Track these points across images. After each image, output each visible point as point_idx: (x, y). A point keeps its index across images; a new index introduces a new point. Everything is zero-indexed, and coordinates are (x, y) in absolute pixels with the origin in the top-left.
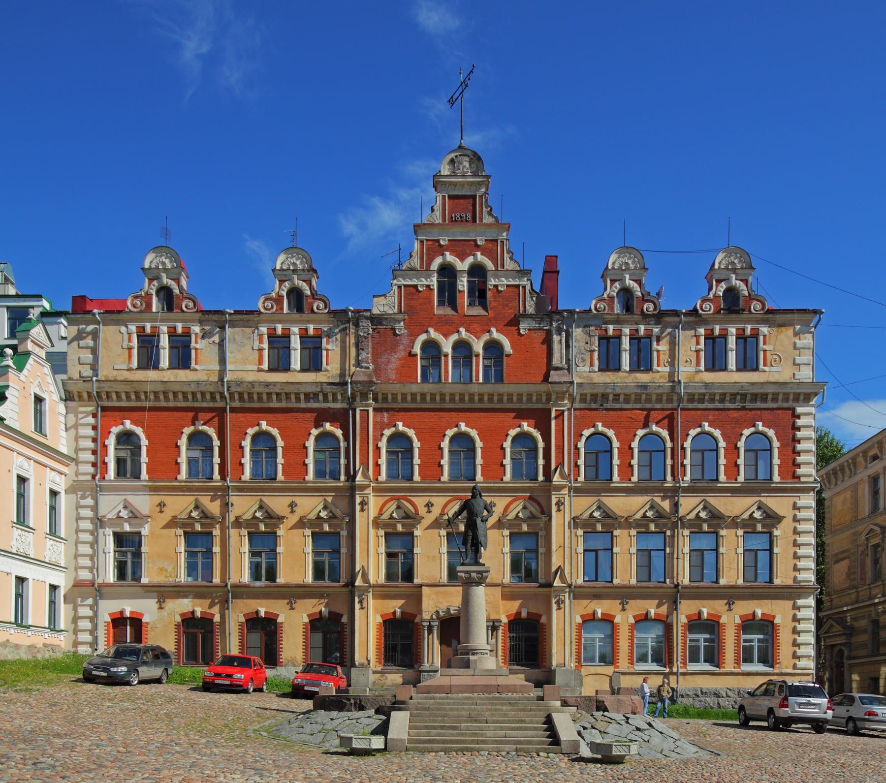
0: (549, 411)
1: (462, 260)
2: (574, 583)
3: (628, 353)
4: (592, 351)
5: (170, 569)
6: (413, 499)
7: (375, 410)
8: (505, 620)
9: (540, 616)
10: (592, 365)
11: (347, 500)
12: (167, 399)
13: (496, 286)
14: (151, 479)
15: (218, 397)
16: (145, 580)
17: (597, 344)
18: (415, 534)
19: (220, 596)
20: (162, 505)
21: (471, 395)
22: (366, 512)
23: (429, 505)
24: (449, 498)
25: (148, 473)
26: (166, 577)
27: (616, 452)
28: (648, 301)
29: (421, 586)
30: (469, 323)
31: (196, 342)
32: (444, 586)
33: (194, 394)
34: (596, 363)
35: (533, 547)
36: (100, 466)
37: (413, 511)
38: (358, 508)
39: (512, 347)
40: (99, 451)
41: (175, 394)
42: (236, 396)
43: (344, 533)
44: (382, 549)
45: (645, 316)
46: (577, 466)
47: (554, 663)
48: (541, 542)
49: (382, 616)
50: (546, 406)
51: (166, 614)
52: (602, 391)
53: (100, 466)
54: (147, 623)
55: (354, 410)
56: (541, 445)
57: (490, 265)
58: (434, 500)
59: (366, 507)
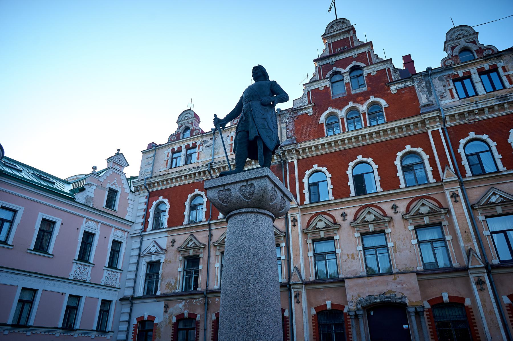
0: (427, 133)
1: (345, 69)
2: (490, 263)
3: (480, 84)
4: (451, 90)
5: (173, 284)
6: (331, 213)
7: (298, 160)
8: (427, 306)
9: (464, 299)
10: (453, 97)
11: (284, 221)
12: (182, 180)
13: (369, 74)
14: (169, 227)
15: (207, 173)
16: (158, 293)
17: (452, 84)
19: (201, 300)
20: (173, 241)
21: (363, 136)
23: (344, 215)
24: (357, 208)
25: (168, 224)
26: (171, 289)
28: (485, 50)
29: (342, 281)
30: (355, 98)
31: (199, 149)
32: (363, 277)
33: (195, 174)
34: (455, 95)
36: (145, 224)
37: (332, 221)
38: (290, 224)
40: (146, 217)
41: (185, 176)
42: (216, 170)
43: (283, 245)
44: (311, 254)
45: (487, 58)
46: (462, 168)
48: (446, 230)
49: (315, 308)
51: (168, 316)
52: (468, 110)
53: (145, 224)
54: (157, 324)
55: (285, 164)
56: (426, 157)
57: (362, 65)
58: (347, 211)
59: (296, 224)
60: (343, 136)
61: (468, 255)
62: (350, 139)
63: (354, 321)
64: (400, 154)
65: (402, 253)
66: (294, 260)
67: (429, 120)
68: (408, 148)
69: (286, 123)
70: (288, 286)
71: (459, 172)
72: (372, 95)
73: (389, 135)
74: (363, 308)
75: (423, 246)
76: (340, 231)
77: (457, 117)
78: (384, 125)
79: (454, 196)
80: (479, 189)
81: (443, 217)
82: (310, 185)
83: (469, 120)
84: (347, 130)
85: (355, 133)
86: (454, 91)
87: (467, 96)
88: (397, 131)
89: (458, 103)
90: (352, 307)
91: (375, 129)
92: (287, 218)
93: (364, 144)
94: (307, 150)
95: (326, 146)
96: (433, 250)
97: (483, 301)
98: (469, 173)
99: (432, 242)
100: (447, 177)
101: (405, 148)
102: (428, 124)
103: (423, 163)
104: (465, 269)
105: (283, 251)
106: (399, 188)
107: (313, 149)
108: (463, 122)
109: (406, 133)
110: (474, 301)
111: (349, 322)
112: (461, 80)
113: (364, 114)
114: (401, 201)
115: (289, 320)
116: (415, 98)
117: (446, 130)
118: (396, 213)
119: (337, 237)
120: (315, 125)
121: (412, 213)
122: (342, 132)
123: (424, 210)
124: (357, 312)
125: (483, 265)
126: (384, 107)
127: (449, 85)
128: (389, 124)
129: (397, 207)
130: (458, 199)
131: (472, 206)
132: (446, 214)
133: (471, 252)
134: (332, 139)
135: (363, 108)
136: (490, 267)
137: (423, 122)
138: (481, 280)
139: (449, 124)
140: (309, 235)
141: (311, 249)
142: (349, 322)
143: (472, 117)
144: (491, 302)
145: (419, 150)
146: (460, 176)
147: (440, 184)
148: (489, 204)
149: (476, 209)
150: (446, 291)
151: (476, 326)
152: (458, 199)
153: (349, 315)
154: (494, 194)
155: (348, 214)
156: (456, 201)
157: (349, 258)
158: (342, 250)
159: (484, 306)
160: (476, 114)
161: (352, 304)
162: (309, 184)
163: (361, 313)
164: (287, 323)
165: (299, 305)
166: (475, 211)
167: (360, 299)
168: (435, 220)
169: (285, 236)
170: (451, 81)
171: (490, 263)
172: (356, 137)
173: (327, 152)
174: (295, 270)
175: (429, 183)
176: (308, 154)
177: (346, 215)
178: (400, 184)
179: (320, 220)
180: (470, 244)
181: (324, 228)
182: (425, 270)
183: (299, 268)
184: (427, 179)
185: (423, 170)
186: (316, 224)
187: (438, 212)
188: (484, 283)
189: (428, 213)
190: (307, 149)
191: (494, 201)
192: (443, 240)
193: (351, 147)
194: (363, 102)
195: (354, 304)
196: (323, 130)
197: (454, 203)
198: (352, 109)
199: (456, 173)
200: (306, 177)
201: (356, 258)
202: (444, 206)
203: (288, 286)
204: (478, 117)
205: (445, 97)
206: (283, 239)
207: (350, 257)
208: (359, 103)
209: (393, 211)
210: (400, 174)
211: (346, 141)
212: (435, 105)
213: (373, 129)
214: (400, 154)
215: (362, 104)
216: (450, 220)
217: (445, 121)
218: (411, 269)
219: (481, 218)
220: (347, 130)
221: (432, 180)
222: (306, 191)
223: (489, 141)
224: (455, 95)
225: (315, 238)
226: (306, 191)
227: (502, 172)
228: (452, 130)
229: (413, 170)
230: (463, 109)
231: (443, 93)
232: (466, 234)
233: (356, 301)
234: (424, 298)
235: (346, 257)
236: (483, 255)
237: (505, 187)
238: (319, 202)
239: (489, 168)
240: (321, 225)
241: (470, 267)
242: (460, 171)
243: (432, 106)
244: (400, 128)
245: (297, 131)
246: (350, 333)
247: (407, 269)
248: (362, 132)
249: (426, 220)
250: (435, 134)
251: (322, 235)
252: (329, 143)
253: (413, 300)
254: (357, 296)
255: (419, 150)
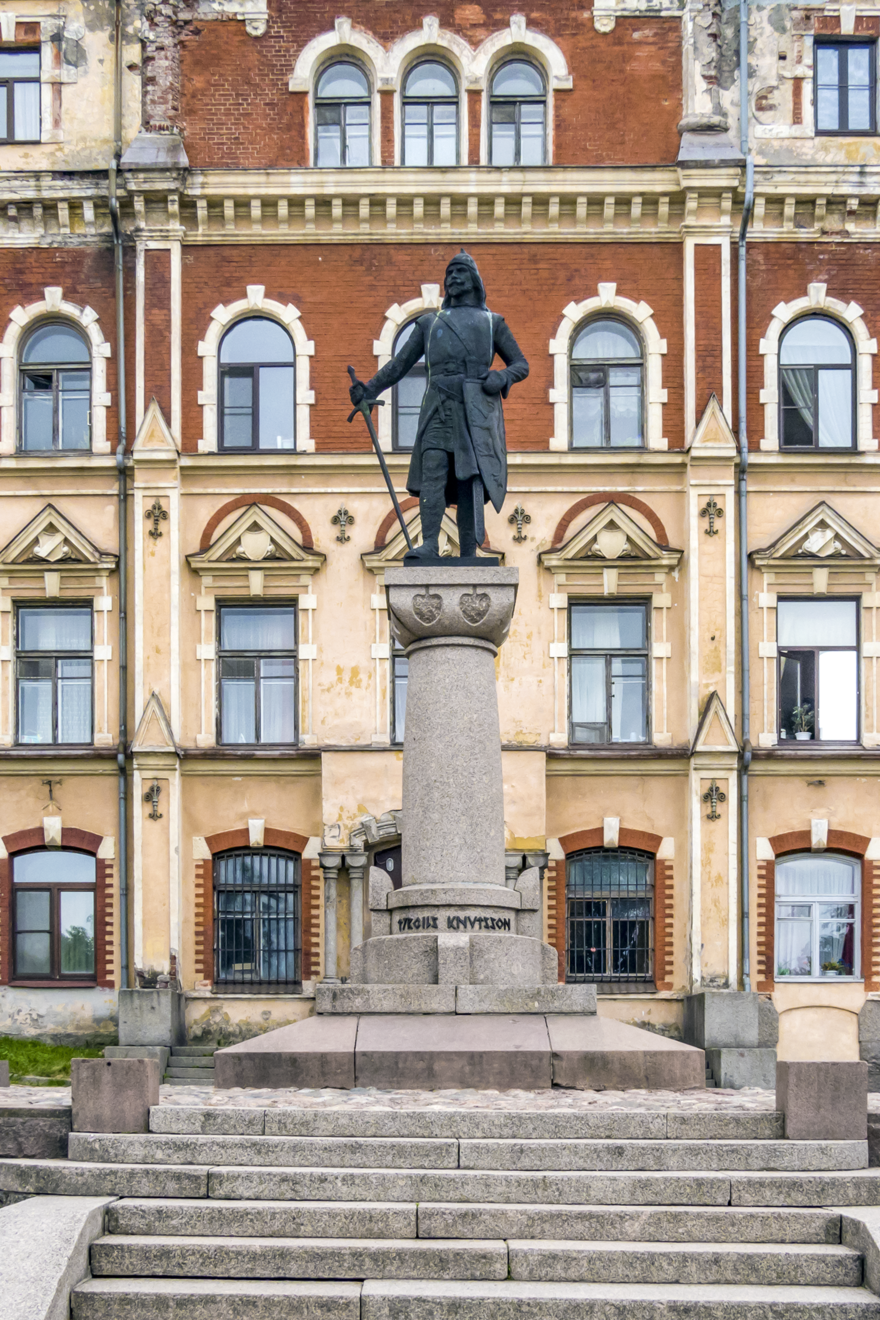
0: (678, 247)
2: (754, 743)
6: (296, 504)
10: (797, 119)
11: (111, 509)
17: (808, 60)
18: (302, 605)
21: (459, 201)
22: (160, 542)
23: (342, 519)
27: (865, 365)
29: (313, 756)
32: (384, 750)
35: (636, 641)
37: (298, 536)
39: (573, 68)
43: (105, 602)
46: (756, 409)
47: (696, 975)
48: (660, 623)
50: (673, 237)
56: (656, 345)
58: (356, 507)
60: (383, 183)
61: (704, 713)
62: (405, 202)
63: (333, 884)
64: (574, 312)
65: (515, 684)
66: (147, 666)
67: (701, 196)
68: (607, 295)
69: (144, 43)
70: (121, 757)
71: (743, 426)
72: (521, 9)
73: (552, 221)
74: (368, 847)
75: (580, 665)
76: (322, 578)
77: (789, 210)
78: (541, 176)
79: (711, 511)
80: (786, 498)
81: (660, 577)
82: (227, 371)
83: (824, 233)
84: (397, 163)
85: (431, 184)
86: (807, 88)
87: (843, 131)
88: (582, 210)
89: (811, 149)
90: (331, 843)
91: (511, 182)
92: (125, 499)
93: (456, 238)
94: (229, 210)
95: (310, 211)
96: (609, 684)
97: (708, 848)
98: (771, 439)
99: (609, 656)
100: (705, 439)
101: (595, 293)
102: (694, 212)
103: (640, 365)
104: (683, 754)
105: (105, 627)
106: (546, 450)
107: (256, 211)
108: (804, 234)
109: (609, 227)
110: (683, 848)
111: (317, 888)
112: (842, 44)
113: (475, 95)
114: (543, 497)
115: (115, 871)
116: (672, 82)
117: (743, 251)
118: (519, 539)
119: (306, 601)
120: (271, 94)
121: (571, 552)
122: (378, 161)
123: (611, 545)
124: (349, 861)
125: (734, 748)
126: (553, 84)
127: (799, 61)
128: (560, 176)
129: (527, 519)
130: (718, 524)
131: (750, 556)
132: (671, 568)
133: (715, 703)
134: (337, 184)
135: (475, 64)
136: (748, 755)
137: (678, 199)
138: (717, 788)
139: (759, 230)
140: (207, 580)
141: (208, 633)
142: (317, 888)
143: (833, 223)
144: (727, 854)
145: (641, 312)
146: (744, 440)
147: (678, 459)
148: (801, 558)
149: (759, 568)
150: (618, 814)
151: (671, 916)
152: (718, 524)
153: (322, 866)
154: (823, 525)
155: (358, 520)
156: (711, 532)
157: (340, 680)
158: (320, 650)
159: (706, 863)
160: (852, 213)
161: (335, 832)
162: (220, 365)
163: (361, 861)
164: (108, 881)
165: (157, 825)
166: (756, 574)
167: (364, 819)
168: (635, 586)
169: (112, 572)
170: (809, 42)
171: (754, 743)
172: (432, 201)
173: (310, 239)
174: (154, 705)
175: (642, 449)
176: (230, 228)
177: (351, 520)
178: (552, 435)
179: (255, 527)
180: (717, 677)
181: (266, 559)
182: (574, 745)
183: (163, 698)
184: (642, 432)
185: (635, 392)
186: (238, 542)
187: (649, 558)
188: (722, 797)
189: (621, 558)
190: (229, 205)
191: (814, 549)
192: (640, 655)
193: (405, 239)
194: (480, 33)
195: (345, 833)
196: (302, 126)
197: (703, 535)
198: (431, 56)
199: (736, 432)
200: (213, 332)
201: (364, 683)
202: (673, 542)
203: (121, 757)
204: (850, 227)
205: (771, 107)
206: (104, 582)
207: (347, 677)
208: (465, 36)
209: (512, 532)
210: (559, 393)
211: (391, 209)
212: (732, 133)
213: (499, 182)
214: (574, 312)
215: (475, 44)
216: (680, 594)
217: (748, 217)
218: (530, 740)
219: (766, 598)
220: (397, 163)
221: (657, 440)
222: (207, 396)
223: (860, 329)
224: (807, 110)
225: (229, 593)
226: (207, 396)
227: (862, 453)
228: (760, 258)
229: (602, 383)
230: (818, 183)
231: (771, 89)
232: (711, 646)
233: (349, 823)
234: (550, 831)
235: (333, 676)
236: (743, 716)
237: (853, 508)
238: (254, 449)
239: (832, 431)
240: (255, 546)
241: (699, 748)
242: (747, 427)
243: (722, 138)
244: (596, 201)
245: (187, 104)
246: (314, 921)
247: (521, 738)
248: (458, 183)
249: (609, 582)
250: (707, 256)
251: (256, 584)
252: (323, 202)
253: (521, 833)
254: (354, 809)
255: (641, 312)
